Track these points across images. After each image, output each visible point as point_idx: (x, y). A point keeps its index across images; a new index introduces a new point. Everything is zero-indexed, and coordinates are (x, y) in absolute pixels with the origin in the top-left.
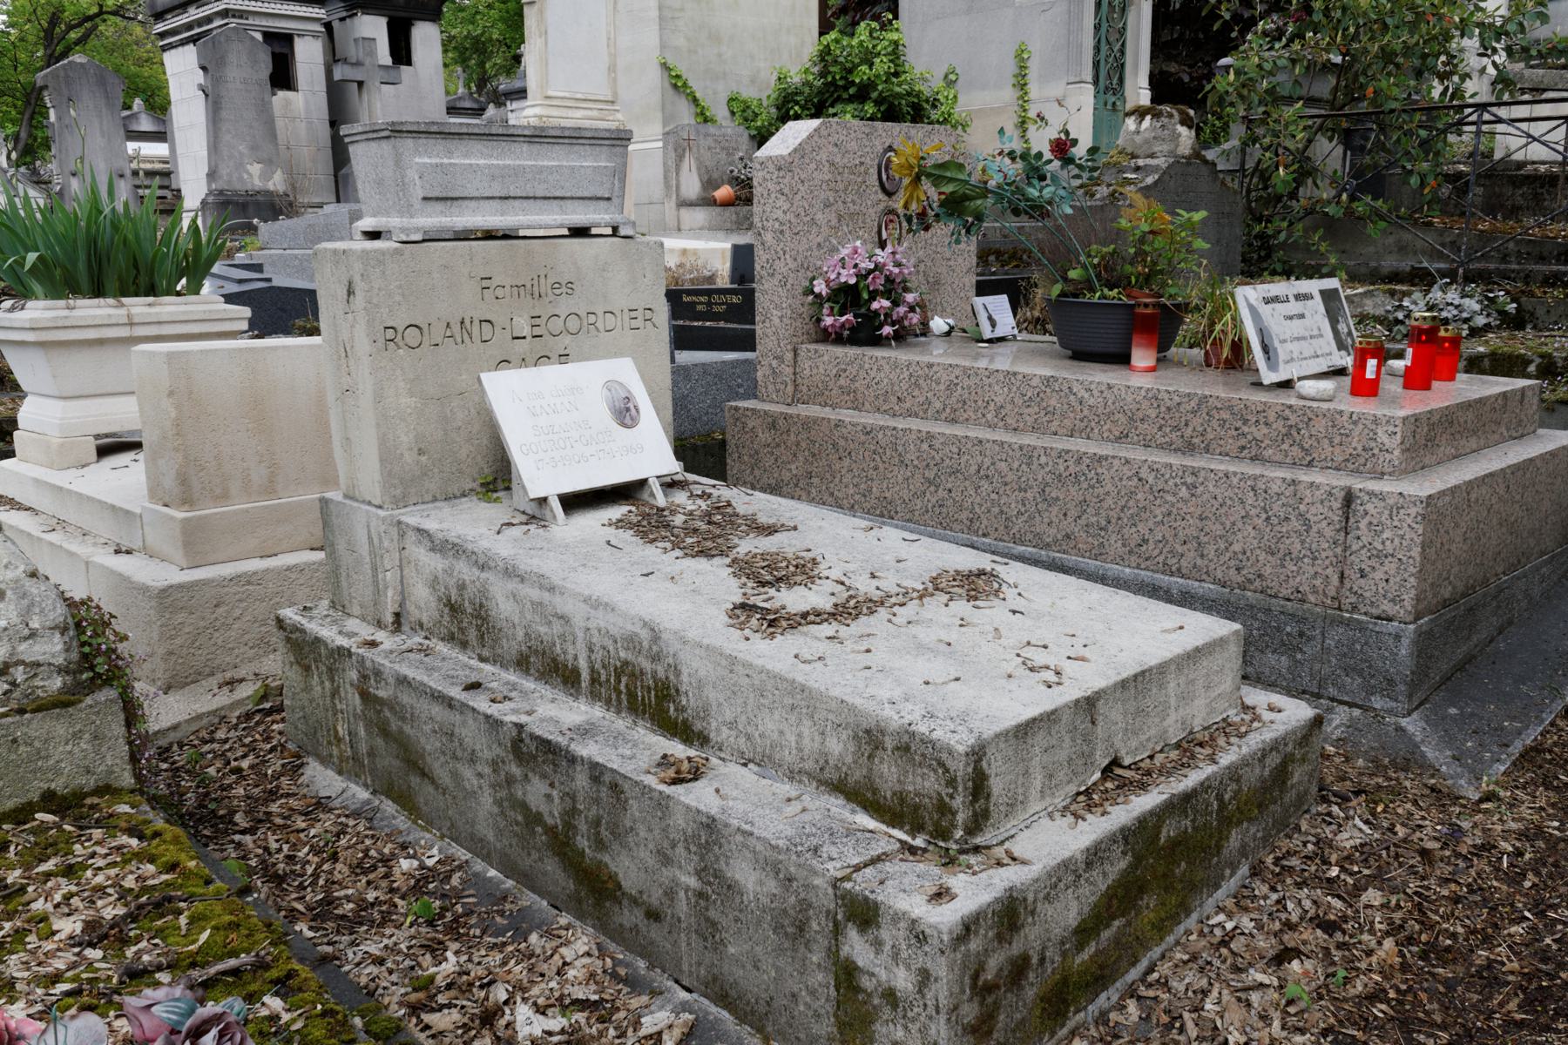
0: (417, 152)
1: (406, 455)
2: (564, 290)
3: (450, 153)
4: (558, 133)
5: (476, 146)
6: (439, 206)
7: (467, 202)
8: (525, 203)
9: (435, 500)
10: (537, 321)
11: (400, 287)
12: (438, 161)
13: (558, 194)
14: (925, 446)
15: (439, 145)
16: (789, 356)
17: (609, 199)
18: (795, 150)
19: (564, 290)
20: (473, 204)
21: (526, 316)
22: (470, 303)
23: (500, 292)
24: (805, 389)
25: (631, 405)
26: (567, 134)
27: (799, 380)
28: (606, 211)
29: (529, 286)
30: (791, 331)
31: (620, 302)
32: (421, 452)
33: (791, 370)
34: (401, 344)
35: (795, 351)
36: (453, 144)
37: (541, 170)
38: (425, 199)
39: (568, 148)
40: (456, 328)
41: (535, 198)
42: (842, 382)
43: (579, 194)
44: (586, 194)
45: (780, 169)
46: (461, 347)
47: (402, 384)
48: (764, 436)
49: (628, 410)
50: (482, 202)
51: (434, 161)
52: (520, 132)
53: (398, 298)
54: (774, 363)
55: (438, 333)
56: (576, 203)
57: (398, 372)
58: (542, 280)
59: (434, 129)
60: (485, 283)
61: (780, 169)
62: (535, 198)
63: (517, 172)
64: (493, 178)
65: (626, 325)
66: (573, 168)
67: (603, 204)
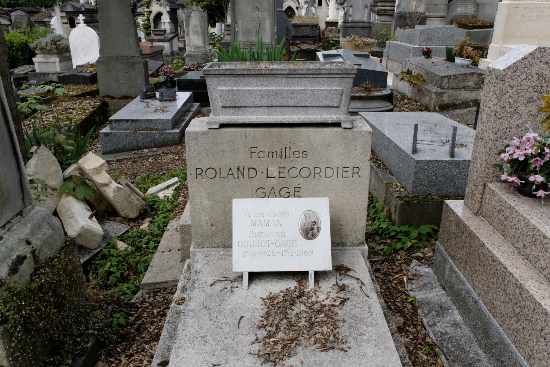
0: (219, 84)
1: (205, 226)
2: (301, 155)
3: (238, 84)
4: (305, 72)
5: (255, 80)
6: (231, 111)
7: (247, 109)
8: (282, 109)
9: (218, 246)
10: (282, 170)
11: (205, 150)
12: (230, 88)
13: (303, 105)
14: (518, 291)
15: (232, 80)
16: (480, 188)
17: (337, 107)
18: (509, 68)
19: (301, 155)
20: (251, 109)
21: (276, 167)
22: (243, 159)
23: (261, 155)
24: (484, 210)
25: (315, 227)
26: (310, 72)
27: (483, 203)
28: (335, 114)
29: (279, 152)
30: (484, 175)
31: (337, 162)
32: (212, 225)
33: (480, 196)
34: (204, 176)
35: (485, 185)
36: (240, 80)
37: (292, 92)
38: (223, 107)
39: (311, 80)
40: (235, 171)
41: (289, 107)
42: (500, 216)
43: (318, 105)
44: (321, 105)
45: (497, 78)
46: (236, 180)
47: (204, 194)
48: (454, 228)
49: (312, 229)
50: (256, 109)
51: (228, 88)
52: (280, 72)
53: (204, 155)
54: (473, 187)
55: (224, 173)
56: (315, 109)
57: (202, 189)
58: (288, 150)
59: (228, 72)
60: (253, 150)
61: (497, 78)
62: (289, 107)
63: (277, 93)
64: (263, 96)
65: (340, 175)
66: (313, 91)
67: (335, 110)
